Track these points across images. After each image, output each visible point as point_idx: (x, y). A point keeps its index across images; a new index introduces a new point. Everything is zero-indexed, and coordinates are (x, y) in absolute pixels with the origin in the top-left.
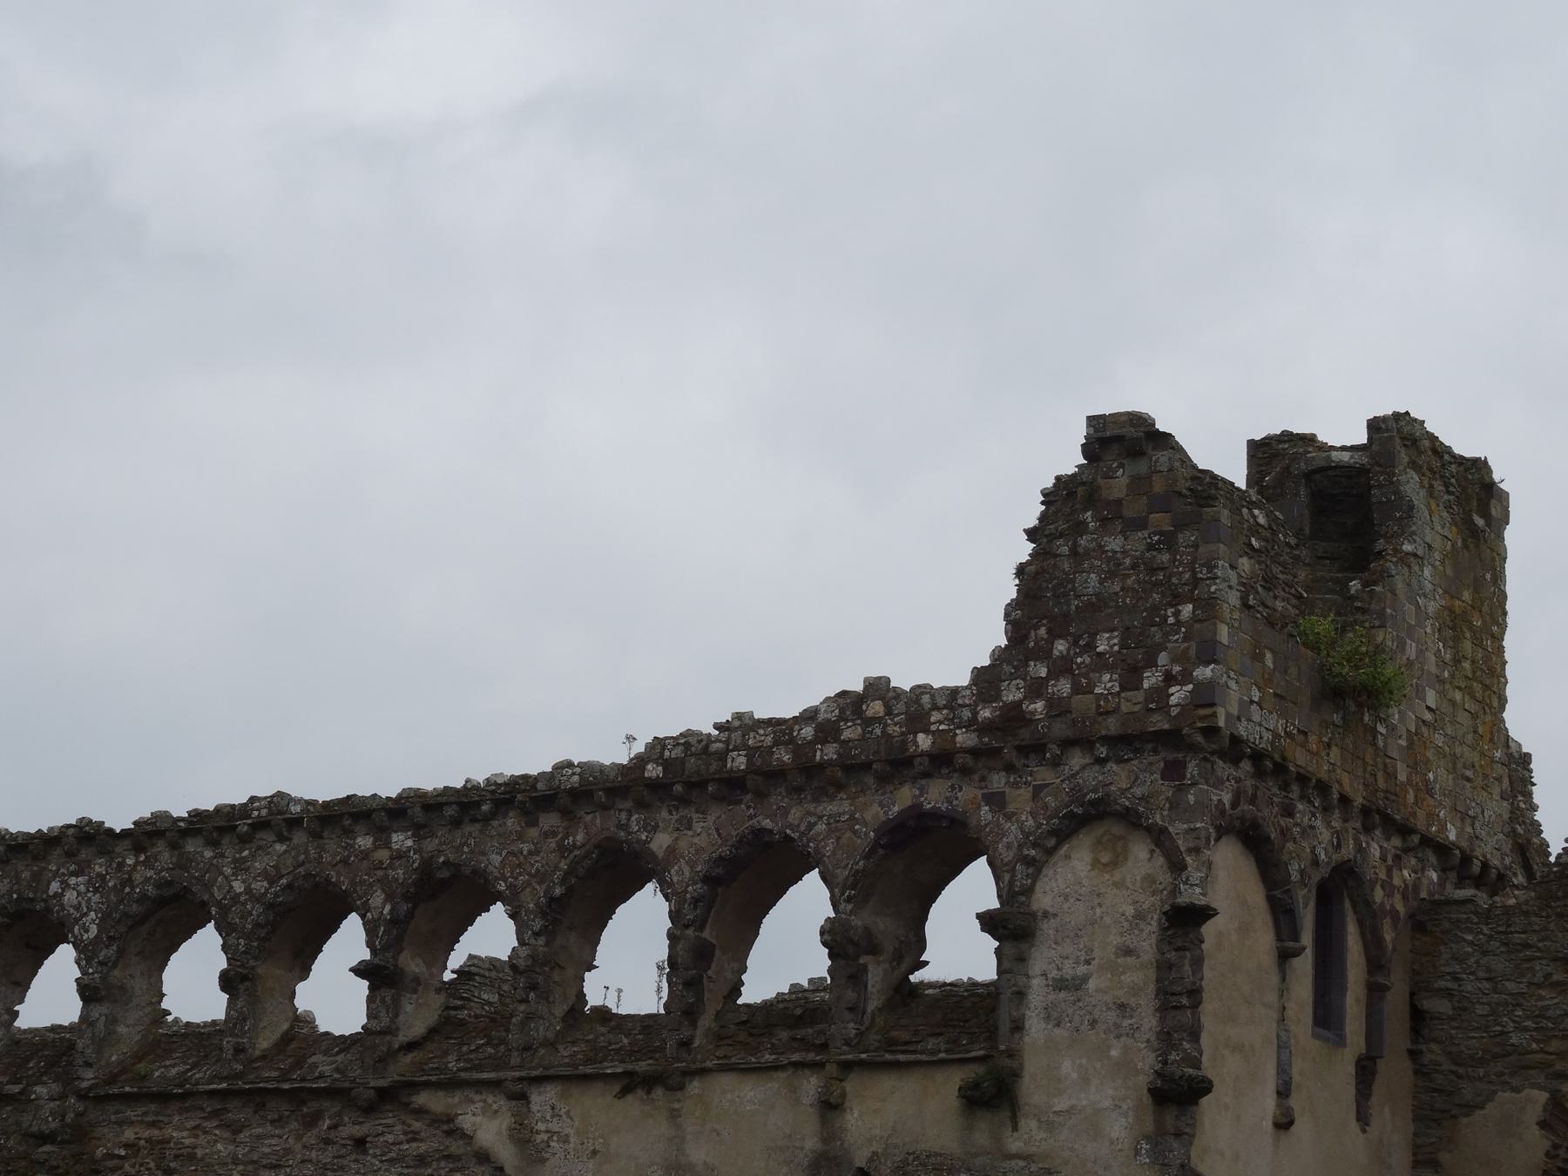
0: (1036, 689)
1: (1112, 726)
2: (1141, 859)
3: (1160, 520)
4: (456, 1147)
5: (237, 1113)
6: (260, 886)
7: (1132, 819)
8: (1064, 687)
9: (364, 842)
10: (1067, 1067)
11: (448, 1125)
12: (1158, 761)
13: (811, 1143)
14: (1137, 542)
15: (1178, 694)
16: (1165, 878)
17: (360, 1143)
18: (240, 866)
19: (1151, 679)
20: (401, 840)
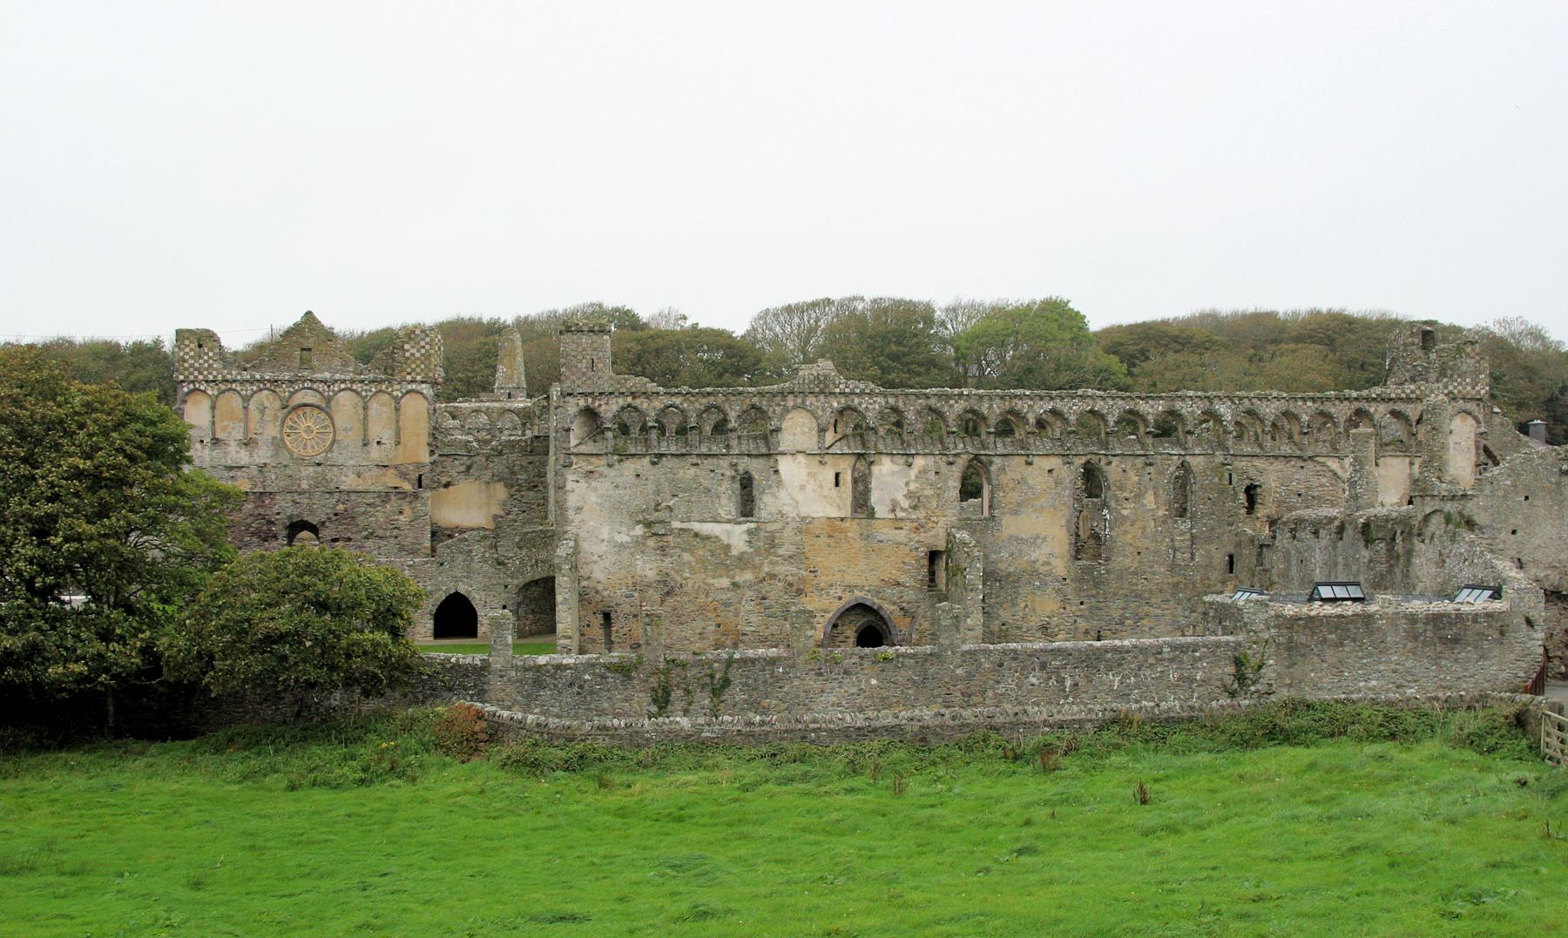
0: (1455, 388)
1: (1469, 397)
2: (1470, 421)
3: (1477, 358)
4: (1324, 469)
5: (1272, 460)
6: (1273, 411)
7: (1469, 413)
8: (1460, 388)
9: (1300, 403)
10: (1459, 459)
11: (1323, 464)
12: (1475, 403)
13: (1408, 471)
14: (1473, 361)
15: (1482, 392)
16: (1475, 425)
17: (1302, 467)
18: (1267, 406)
19: (1477, 388)
20: (1309, 404)
